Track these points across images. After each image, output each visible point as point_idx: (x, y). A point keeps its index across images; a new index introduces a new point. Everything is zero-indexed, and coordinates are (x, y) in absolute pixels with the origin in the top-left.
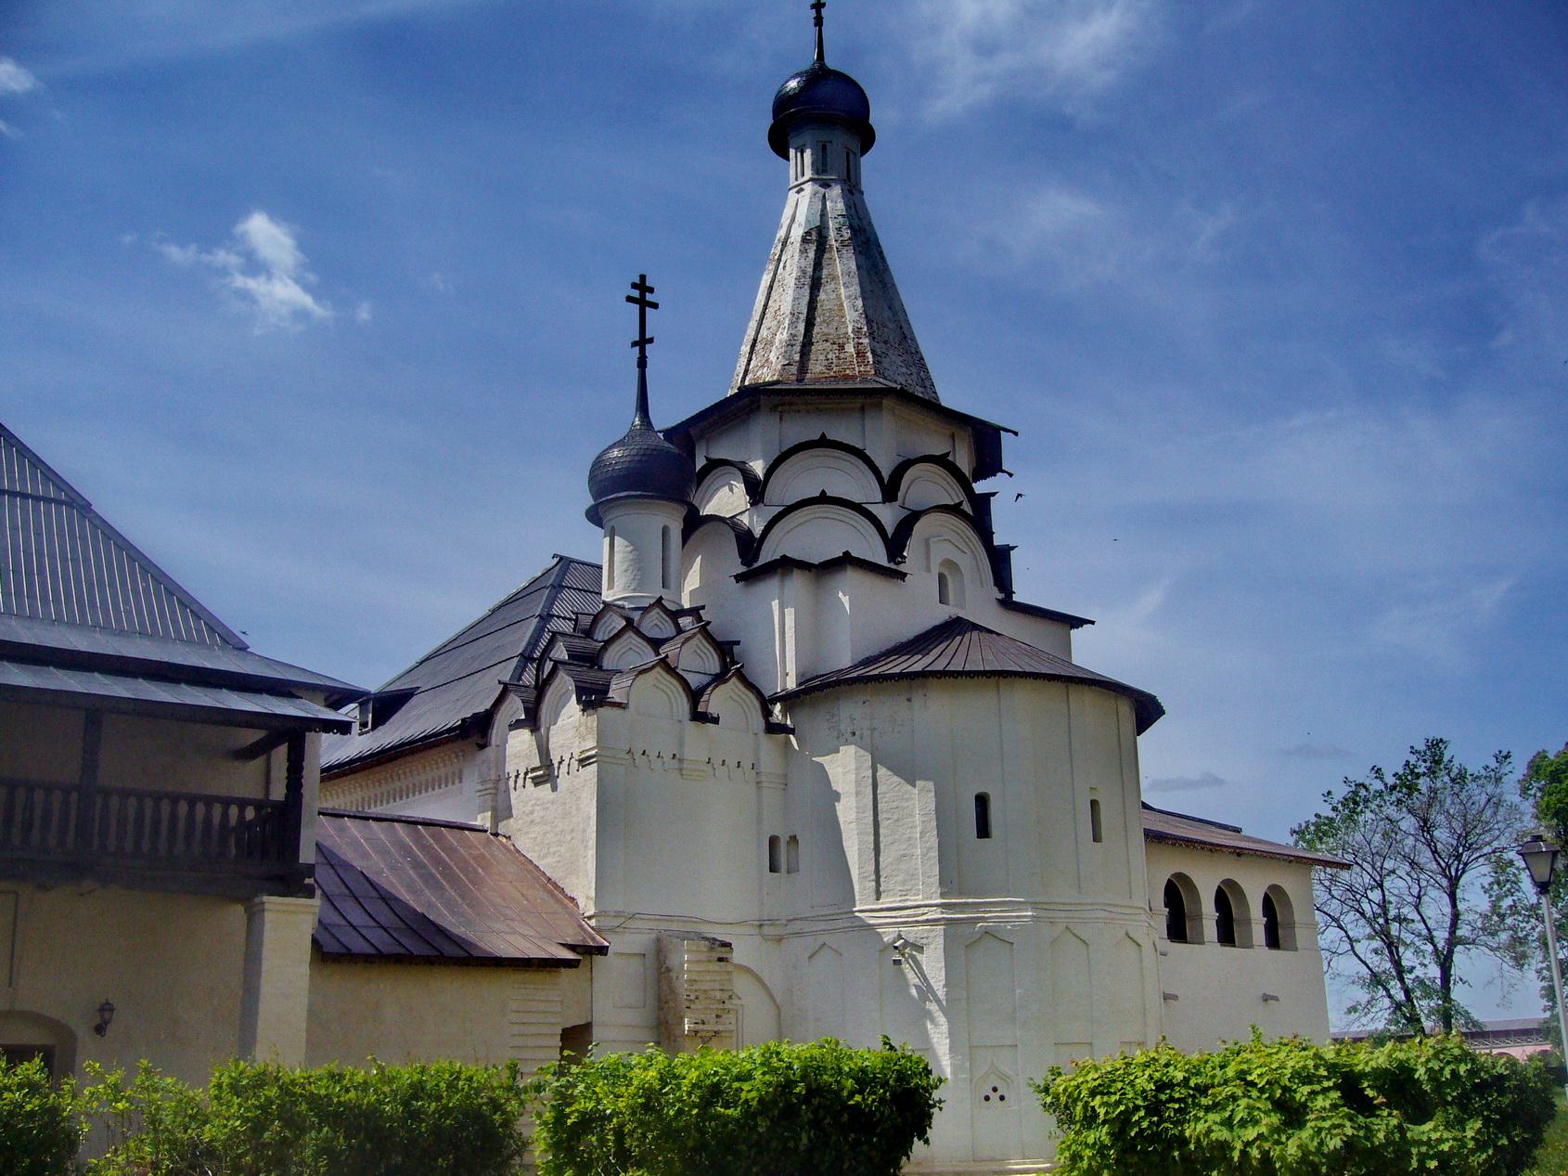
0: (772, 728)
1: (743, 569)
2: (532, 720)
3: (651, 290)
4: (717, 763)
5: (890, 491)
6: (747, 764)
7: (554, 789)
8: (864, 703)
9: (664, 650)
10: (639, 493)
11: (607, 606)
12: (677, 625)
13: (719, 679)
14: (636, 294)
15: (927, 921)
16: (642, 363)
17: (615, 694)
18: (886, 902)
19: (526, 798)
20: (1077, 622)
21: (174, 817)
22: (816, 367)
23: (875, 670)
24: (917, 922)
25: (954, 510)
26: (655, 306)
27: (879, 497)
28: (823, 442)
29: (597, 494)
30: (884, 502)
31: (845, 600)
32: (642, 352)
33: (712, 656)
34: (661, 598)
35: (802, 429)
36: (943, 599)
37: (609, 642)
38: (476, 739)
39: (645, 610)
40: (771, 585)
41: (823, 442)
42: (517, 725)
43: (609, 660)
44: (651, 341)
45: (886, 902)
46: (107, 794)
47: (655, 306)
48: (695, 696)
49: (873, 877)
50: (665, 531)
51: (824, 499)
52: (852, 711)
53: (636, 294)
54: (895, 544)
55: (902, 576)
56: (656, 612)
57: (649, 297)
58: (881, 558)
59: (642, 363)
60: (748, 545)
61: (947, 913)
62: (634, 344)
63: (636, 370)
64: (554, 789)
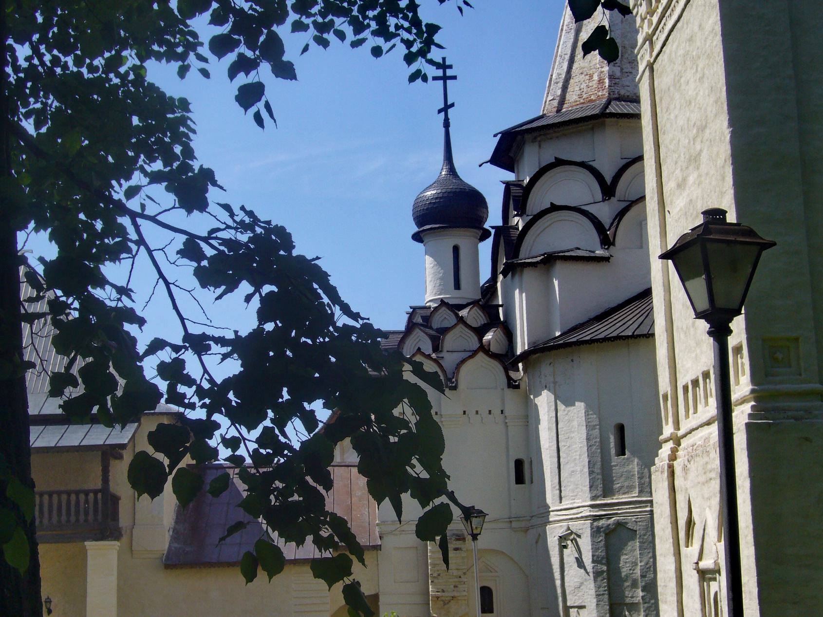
4: (471, 412)
6: (496, 412)
8: (550, 364)
10: (437, 226)
12: (457, 315)
13: (474, 353)
15: (582, 517)
16: (447, 124)
18: (566, 504)
21: (87, 501)
22: (572, 97)
23: (586, 335)
24: (577, 518)
33: (473, 337)
35: (549, 152)
41: (559, 163)
45: (566, 504)
46: (41, 495)
49: (558, 487)
59: (447, 124)
61: (593, 512)
63: (443, 130)
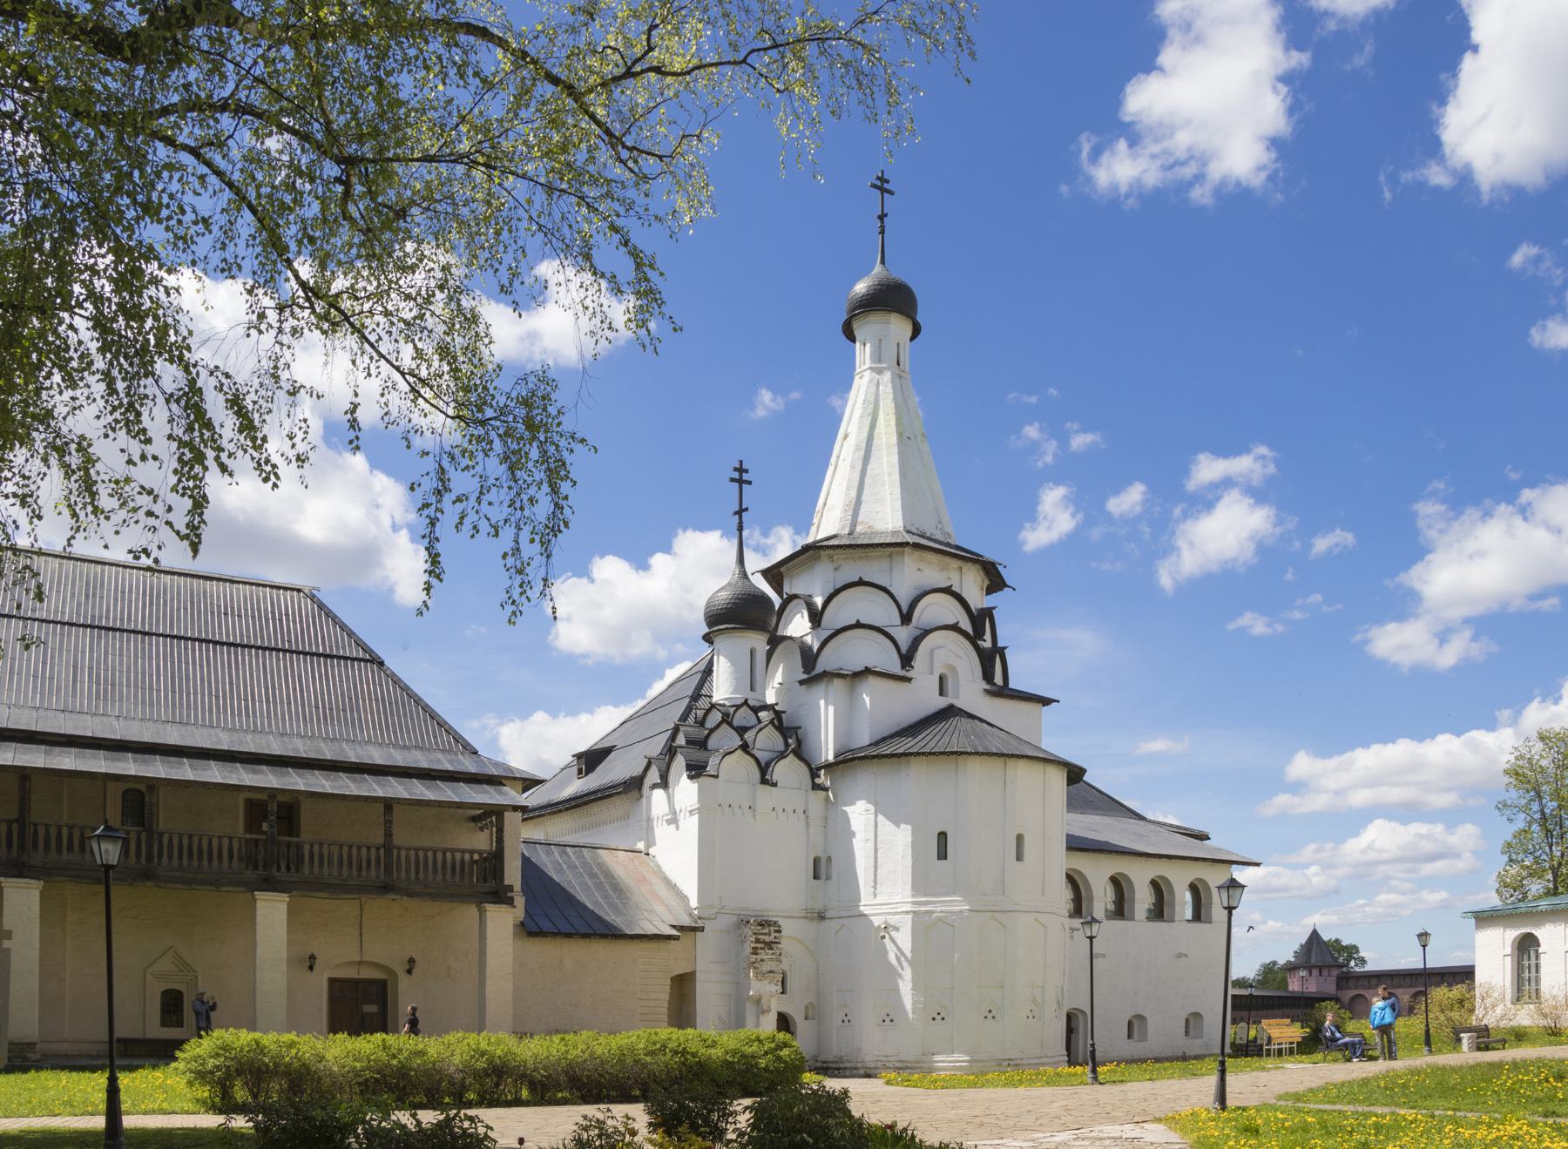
0: (816, 787)
1: (805, 676)
2: (664, 783)
3: (747, 471)
5: (906, 618)
7: (677, 828)
9: (749, 736)
11: (713, 706)
13: (782, 756)
14: (736, 475)
17: (710, 769)
19: (662, 831)
20: (1046, 701)
25: (955, 628)
26: (749, 483)
27: (898, 621)
28: (861, 583)
29: (710, 625)
30: (903, 624)
31: (867, 699)
32: (741, 518)
34: (746, 700)
36: (941, 694)
37: (712, 731)
38: (635, 793)
39: (738, 707)
40: (819, 689)
41: (861, 583)
42: (655, 786)
43: (712, 743)
44: (746, 509)
47: (749, 483)
48: (764, 769)
50: (752, 652)
51: (859, 625)
52: (865, 778)
53: (736, 475)
54: (907, 660)
55: (909, 680)
56: (745, 707)
57: (745, 476)
58: (896, 668)
60: (809, 658)
62: (736, 513)
64: (677, 828)
